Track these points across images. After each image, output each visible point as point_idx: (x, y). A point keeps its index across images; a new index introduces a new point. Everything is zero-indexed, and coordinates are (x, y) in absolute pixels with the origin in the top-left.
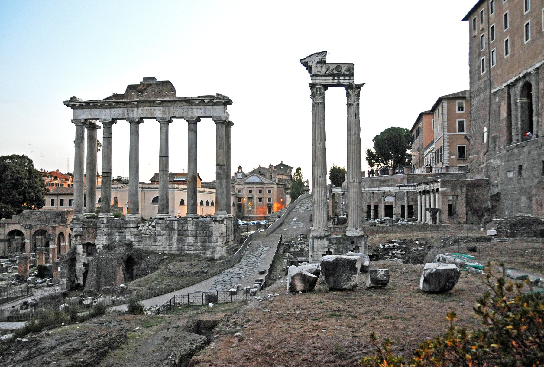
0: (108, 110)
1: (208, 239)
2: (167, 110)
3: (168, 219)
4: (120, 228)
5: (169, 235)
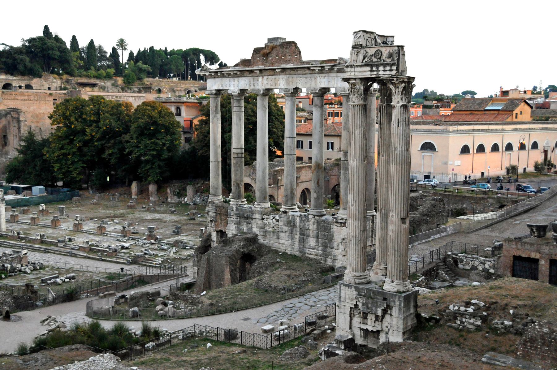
0: (236, 79)
1: (330, 243)
2: (290, 79)
5: (292, 233)
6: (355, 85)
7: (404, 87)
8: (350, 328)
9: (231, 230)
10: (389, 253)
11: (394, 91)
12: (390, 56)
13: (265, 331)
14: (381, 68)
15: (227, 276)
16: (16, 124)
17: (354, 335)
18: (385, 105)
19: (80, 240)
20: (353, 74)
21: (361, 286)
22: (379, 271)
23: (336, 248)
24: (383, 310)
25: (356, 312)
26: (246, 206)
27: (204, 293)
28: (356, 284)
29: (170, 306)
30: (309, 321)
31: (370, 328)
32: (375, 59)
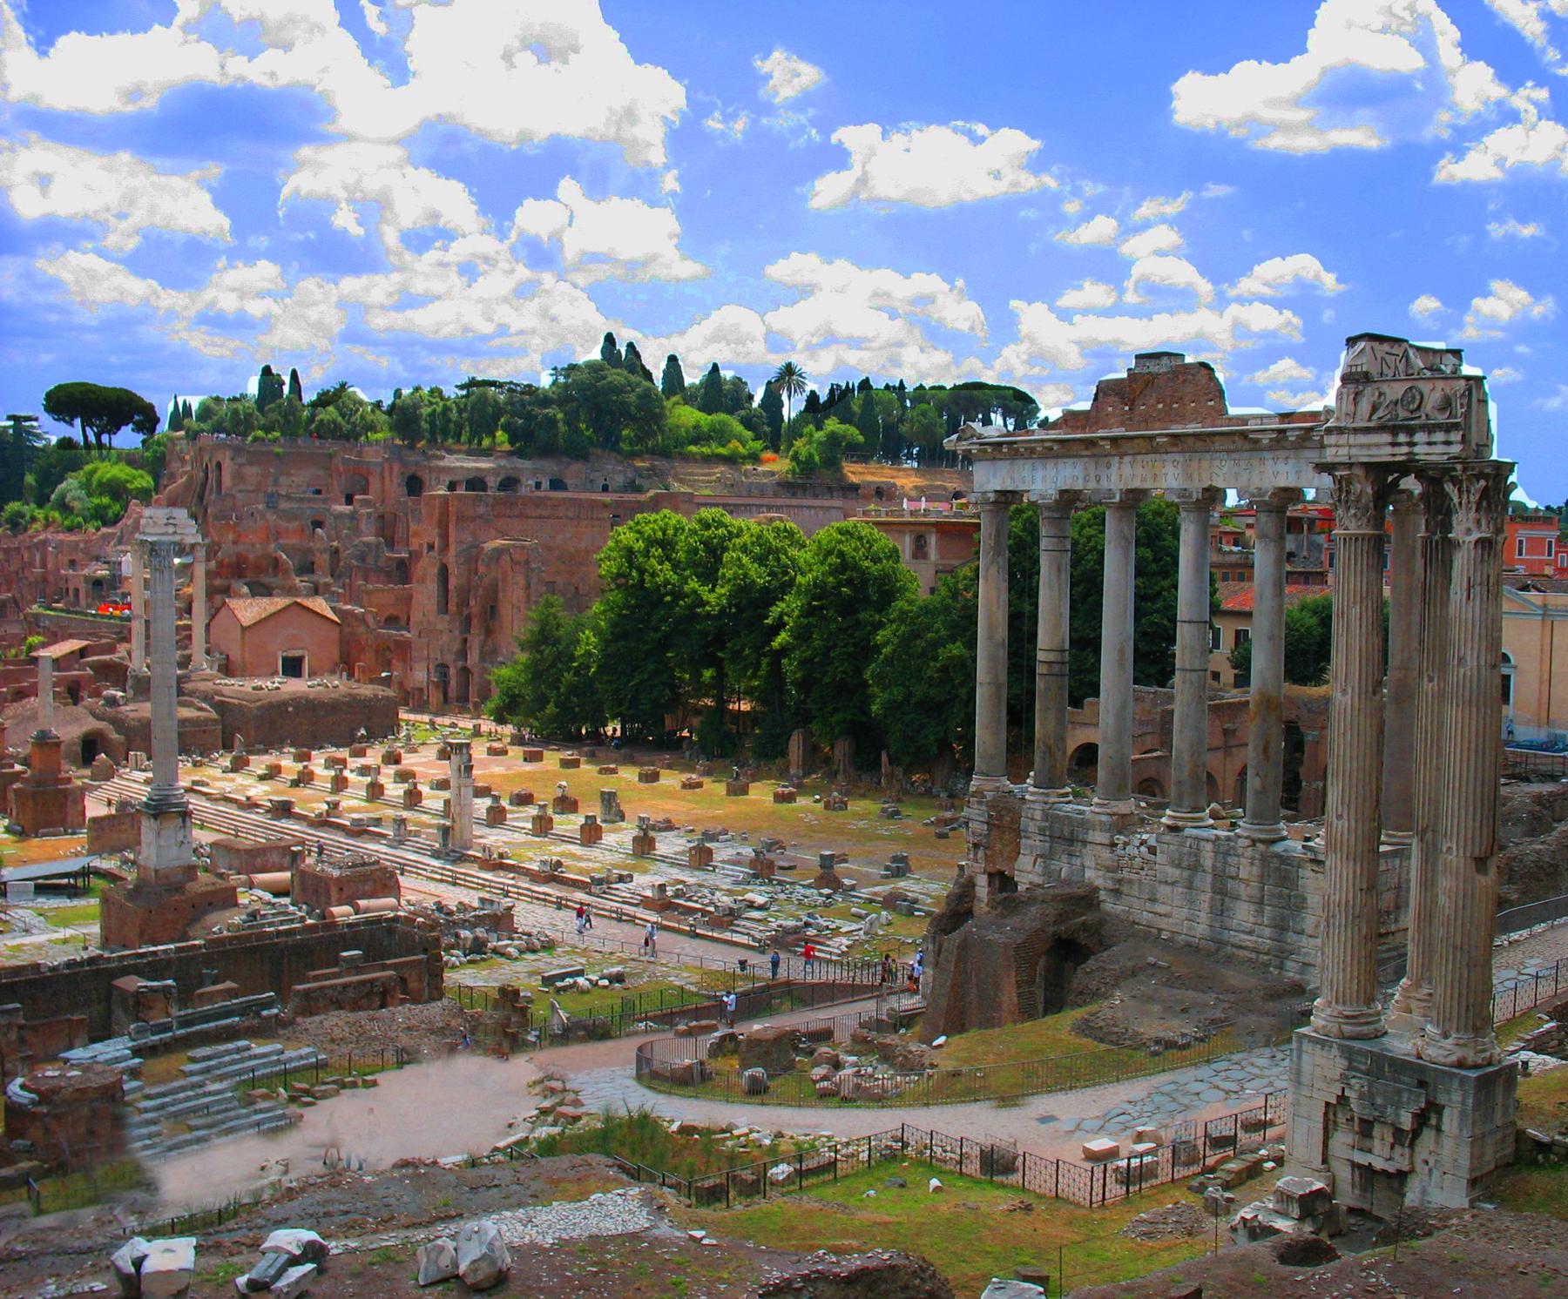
0: (1050, 464)
2: (1195, 464)
3: (1188, 832)
4: (1071, 841)
6: (1349, 483)
7: (1485, 494)
8: (1325, 1161)
9: (1027, 872)
10: (1437, 956)
11: (1456, 500)
12: (1446, 404)
13: (1092, 1156)
14: (1420, 437)
15: (1009, 996)
16: (521, 580)
17: (1333, 1183)
18: (1436, 538)
19: (644, 882)
20: (1344, 451)
21: (1357, 1045)
22: (1414, 1005)
23: (1310, 932)
24: (1415, 1116)
25: (1341, 1119)
26: (1069, 807)
27: (942, 1040)
28: (1344, 1038)
29: (849, 1071)
30: (1215, 1134)
31: (1379, 1164)
32: (1402, 414)
